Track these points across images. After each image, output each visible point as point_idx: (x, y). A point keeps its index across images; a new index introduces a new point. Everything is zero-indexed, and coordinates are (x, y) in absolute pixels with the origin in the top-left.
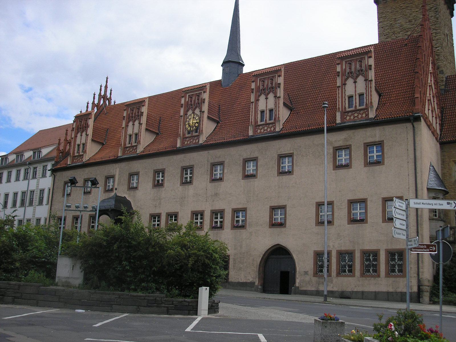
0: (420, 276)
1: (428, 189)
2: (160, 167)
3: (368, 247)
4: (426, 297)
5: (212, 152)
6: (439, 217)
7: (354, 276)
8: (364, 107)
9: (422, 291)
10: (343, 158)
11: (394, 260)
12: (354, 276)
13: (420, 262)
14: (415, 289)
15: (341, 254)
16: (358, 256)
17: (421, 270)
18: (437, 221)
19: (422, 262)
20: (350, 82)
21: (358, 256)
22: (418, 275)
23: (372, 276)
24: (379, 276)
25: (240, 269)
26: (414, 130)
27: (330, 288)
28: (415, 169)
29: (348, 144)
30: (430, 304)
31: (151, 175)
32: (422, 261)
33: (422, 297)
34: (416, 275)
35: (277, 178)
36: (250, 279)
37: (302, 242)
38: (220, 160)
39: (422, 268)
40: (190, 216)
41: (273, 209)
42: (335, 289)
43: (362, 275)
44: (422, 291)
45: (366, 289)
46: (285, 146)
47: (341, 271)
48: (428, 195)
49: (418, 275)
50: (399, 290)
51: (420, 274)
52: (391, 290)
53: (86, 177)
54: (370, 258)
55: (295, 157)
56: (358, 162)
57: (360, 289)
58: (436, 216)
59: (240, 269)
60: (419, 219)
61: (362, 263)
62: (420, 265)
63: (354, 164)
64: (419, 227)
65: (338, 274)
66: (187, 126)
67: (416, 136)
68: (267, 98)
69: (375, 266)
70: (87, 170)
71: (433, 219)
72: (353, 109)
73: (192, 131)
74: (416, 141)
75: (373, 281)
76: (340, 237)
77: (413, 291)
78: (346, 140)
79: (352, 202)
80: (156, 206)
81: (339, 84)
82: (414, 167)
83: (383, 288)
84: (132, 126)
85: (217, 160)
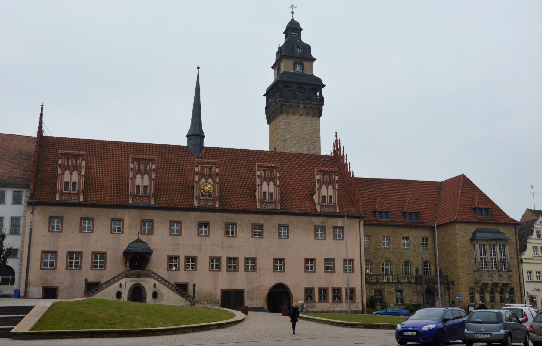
2: (176, 219)
3: (335, 286)
5: (225, 214)
7: (328, 302)
8: (332, 204)
12: (328, 302)
24: (342, 302)
25: (253, 299)
27: (314, 310)
29: (324, 225)
31: (167, 224)
35: (278, 240)
36: (260, 305)
37: (296, 281)
38: (233, 221)
40: (208, 260)
41: (276, 260)
42: (318, 310)
43: (333, 302)
45: (335, 310)
46: (284, 220)
50: (353, 310)
53: (84, 216)
54: (337, 292)
55: (290, 228)
57: (332, 309)
59: (253, 299)
65: (319, 302)
66: (202, 191)
68: (268, 185)
70: (85, 210)
72: (326, 204)
73: (206, 196)
75: (339, 305)
76: (320, 279)
78: (322, 222)
80: (173, 250)
83: (345, 309)
84: (141, 179)
85: (229, 221)
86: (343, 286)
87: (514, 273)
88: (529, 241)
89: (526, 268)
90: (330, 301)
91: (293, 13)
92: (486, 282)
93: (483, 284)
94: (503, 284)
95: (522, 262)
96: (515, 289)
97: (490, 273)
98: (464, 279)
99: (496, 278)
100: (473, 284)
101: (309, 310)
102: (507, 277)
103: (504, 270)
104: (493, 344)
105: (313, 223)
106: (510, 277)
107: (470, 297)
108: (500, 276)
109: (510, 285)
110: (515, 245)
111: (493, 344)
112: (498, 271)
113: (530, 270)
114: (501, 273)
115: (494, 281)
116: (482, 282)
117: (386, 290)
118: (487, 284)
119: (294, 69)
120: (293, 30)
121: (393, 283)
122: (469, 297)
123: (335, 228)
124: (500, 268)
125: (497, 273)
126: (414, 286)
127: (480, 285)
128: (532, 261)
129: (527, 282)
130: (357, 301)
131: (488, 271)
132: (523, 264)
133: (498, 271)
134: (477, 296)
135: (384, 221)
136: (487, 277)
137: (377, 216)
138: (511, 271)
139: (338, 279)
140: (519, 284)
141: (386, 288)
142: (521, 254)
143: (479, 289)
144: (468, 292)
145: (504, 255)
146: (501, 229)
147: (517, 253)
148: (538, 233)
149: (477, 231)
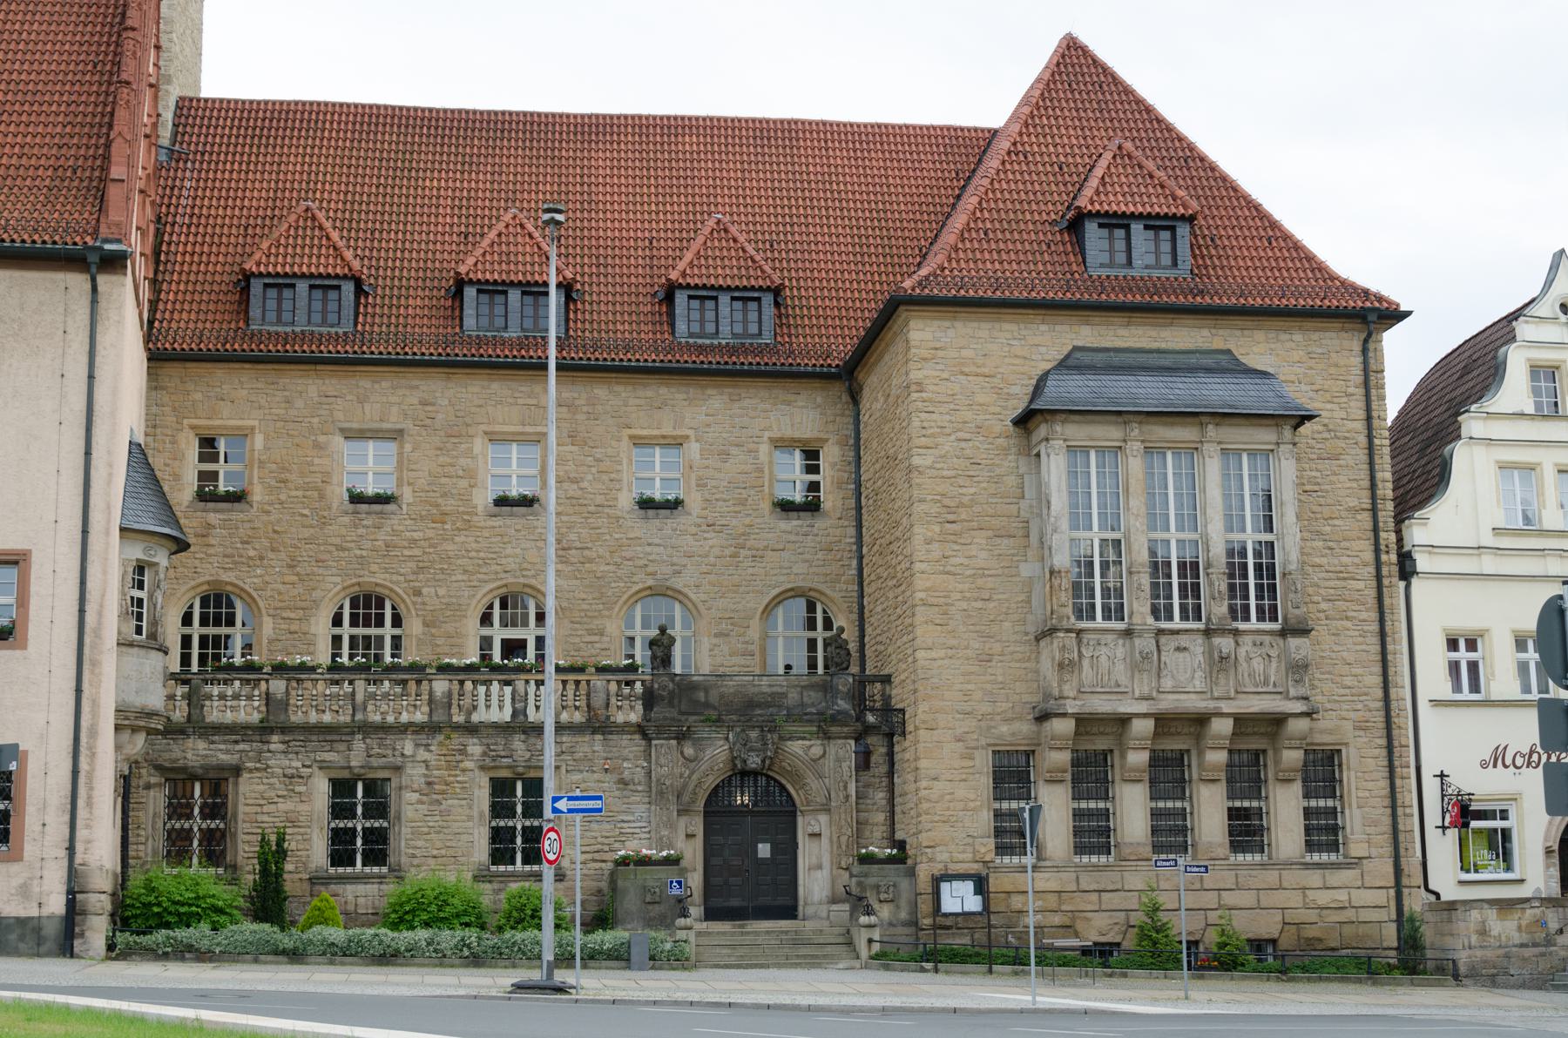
0: (78, 859)
1: (122, 529)
6: (153, 636)
9: (84, 913)
13: (81, 803)
14: (56, 905)
17: (81, 834)
18: (142, 652)
19: (90, 804)
22: (71, 850)
26: (94, 301)
28: (88, 453)
30: (109, 958)
32: (90, 797)
33: (82, 935)
34: (63, 853)
39: (88, 827)
44: (84, 913)
48: (121, 553)
49: (71, 850)
51: (79, 847)
58: (139, 630)
60: (87, 640)
62: (82, 813)
64: (86, 667)
67: (99, 328)
71: (131, 645)
74: (99, 347)
77: (46, 912)
82: (82, 443)
87: (1341, 648)
88: (1472, 424)
89: (1434, 609)
92: (1102, 705)
93: (1085, 722)
94: (1240, 720)
95: (1407, 569)
96: (1350, 756)
97: (1145, 643)
98: (958, 689)
99: (1185, 680)
100: (1026, 727)
102: (1275, 671)
103: (1254, 623)
106: (1299, 669)
107: (998, 815)
108: (1221, 664)
109: (1297, 726)
110: (1363, 456)
112: (1208, 633)
113: (1464, 623)
114: (1224, 643)
115: (1167, 703)
116: (1072, 707)
117: (415, 774)
118: (1123, 721)
121: (471, 729)
122: (985, 820)
124: (1221, 609)
125: (1197, 645)
126: (630, 746)
127: (1064, 727)
128: (1489, 564)
129: (1436, 703)
130: (29, 850)
131: (1128, 633)
132: (1415, 581)
133: (1208, 633)
134: (1055, 809)
135: (510, 344)
136: (1121, 673)
137: (469, 311)
138: (1303, 631)
140: (1380, 717)
141: (417, 762)
142: (1400, 518)
143: (1063, 758)
144: (986, 781)
145: (1269, 528)
146: (1257, 347)
147: (1374, 510)
148: (1544, 374)
149: (1069, 364)
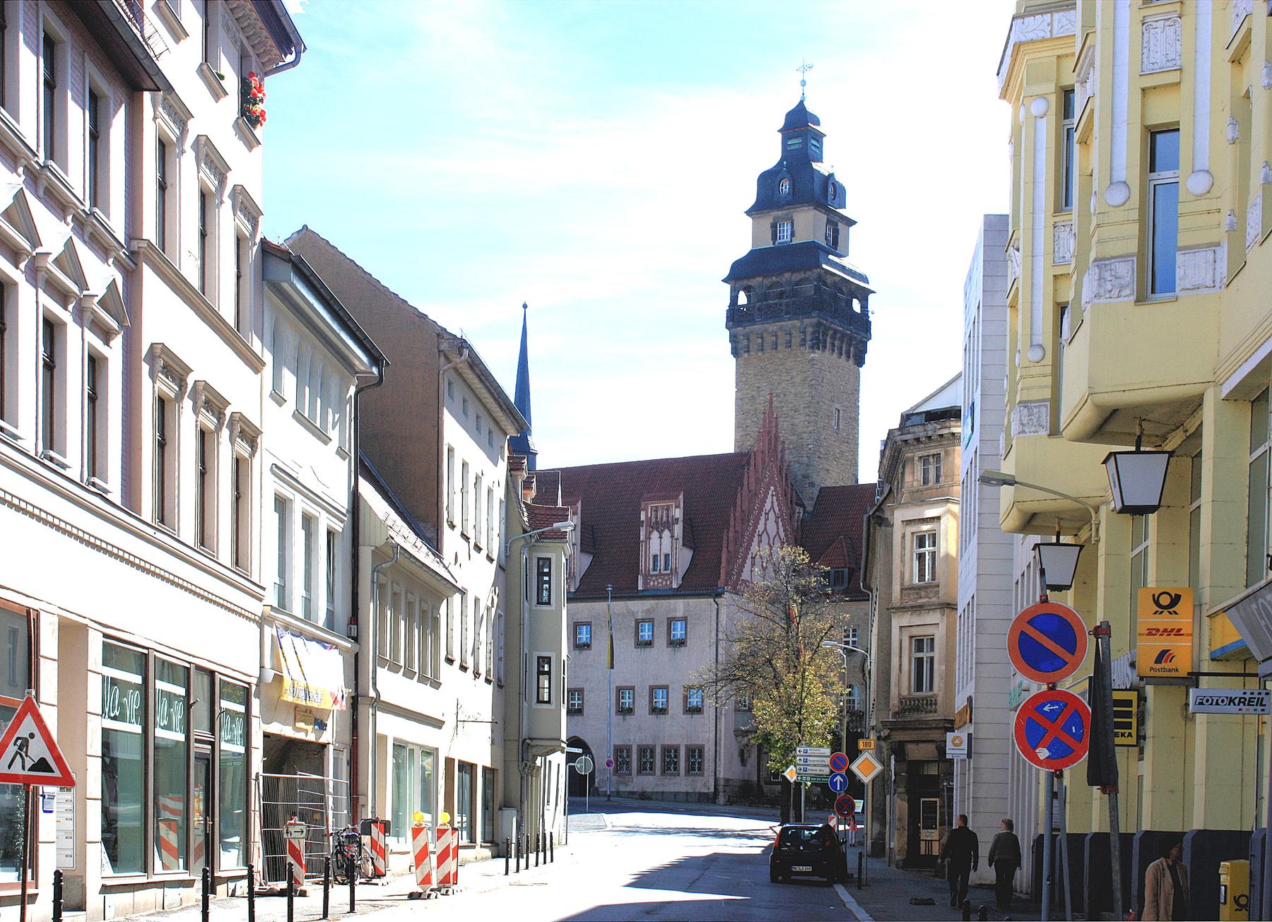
4: (721, 799)
10: (646, 635)
11: (693, 756)
15: (642, 750)
16: (658, 750)
20: (655, 534)
21: (658, 750)
23: (672, 775)
27: (629, 789)
47: (642, 769)
52: (690, 790)
54: (670, 753)
56: (661, 642)
61: (663, 760)
63: (656, 643)
65: (639, 772)
69: (675, 763)
79: (652, 689)
81: (642, 538)
83: (683, 789)
86: (682, 742)
90: (658, 772)
91: (803, 83)
101: (622, 788)
104: (809, 869)
105: (633, 614)
111: (809, 869)
119: (774, 238)
120: (800, 127)
123: (671, 621)
139: (676, 730)
